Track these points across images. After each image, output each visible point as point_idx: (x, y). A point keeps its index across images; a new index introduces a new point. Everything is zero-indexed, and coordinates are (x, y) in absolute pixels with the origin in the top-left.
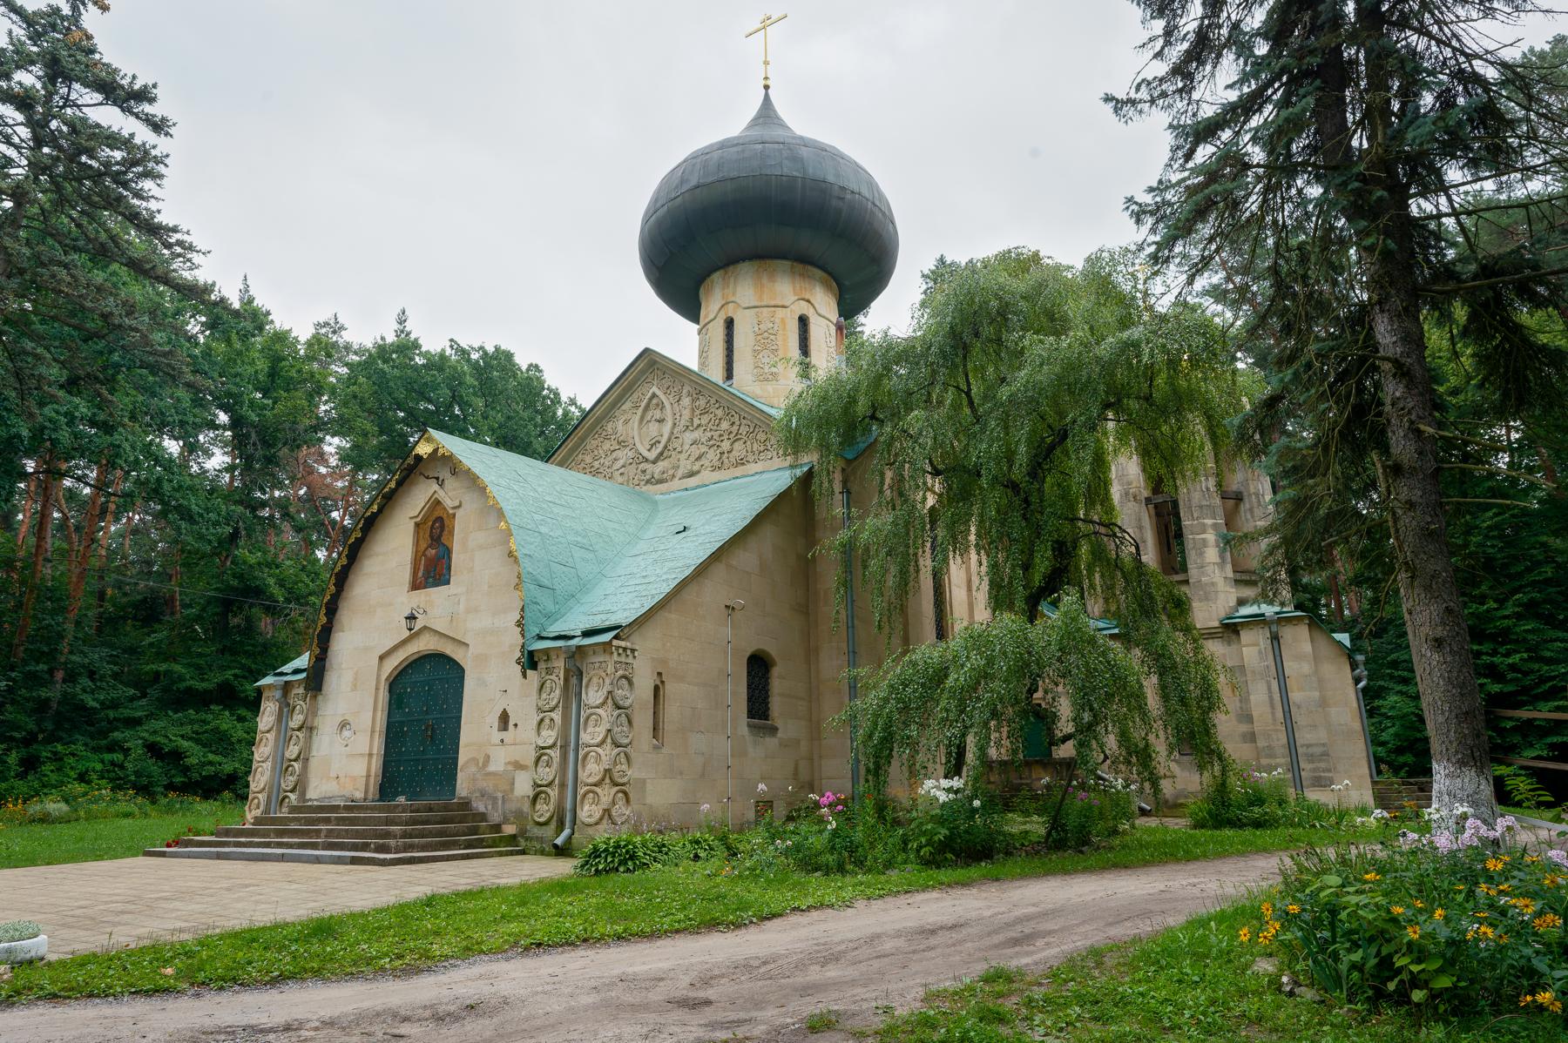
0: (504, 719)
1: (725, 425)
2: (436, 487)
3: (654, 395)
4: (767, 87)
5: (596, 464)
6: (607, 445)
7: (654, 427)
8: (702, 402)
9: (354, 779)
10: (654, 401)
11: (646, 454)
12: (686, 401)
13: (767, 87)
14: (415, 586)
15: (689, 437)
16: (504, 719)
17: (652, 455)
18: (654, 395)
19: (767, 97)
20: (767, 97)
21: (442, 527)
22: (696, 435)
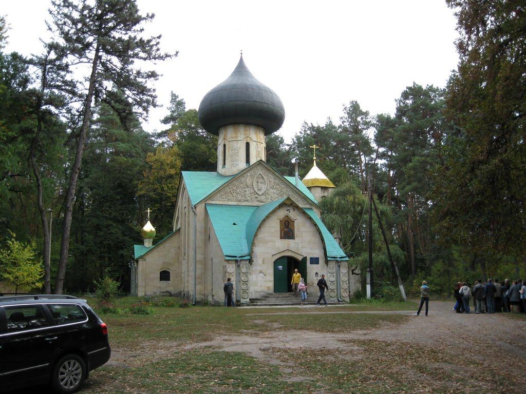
0: (317, 273)
1: (284, 190)
2: (288, 212)
3: (260, 174)
4: (241, 54)
5: (238, 191)
6: (242, 185)
7: (260, 185)
8: (277, 181)
9: (268, 287)
10: (260, 175)
11: (257, 192)
12: (272, 180)
13: (241, 54)
14: (281, 238)
15: (272, 190)
16: (317, 273)
17: (260, 193)
18: (260, 174)
19: (241, 60)
20: (241, 60)
21: (288, 222)
22: (275, 191)
